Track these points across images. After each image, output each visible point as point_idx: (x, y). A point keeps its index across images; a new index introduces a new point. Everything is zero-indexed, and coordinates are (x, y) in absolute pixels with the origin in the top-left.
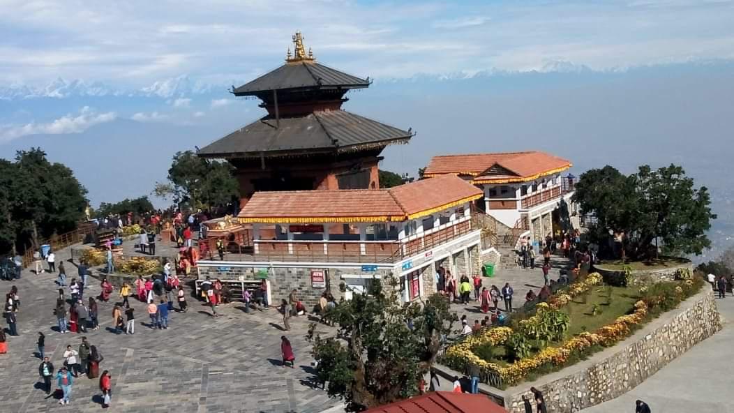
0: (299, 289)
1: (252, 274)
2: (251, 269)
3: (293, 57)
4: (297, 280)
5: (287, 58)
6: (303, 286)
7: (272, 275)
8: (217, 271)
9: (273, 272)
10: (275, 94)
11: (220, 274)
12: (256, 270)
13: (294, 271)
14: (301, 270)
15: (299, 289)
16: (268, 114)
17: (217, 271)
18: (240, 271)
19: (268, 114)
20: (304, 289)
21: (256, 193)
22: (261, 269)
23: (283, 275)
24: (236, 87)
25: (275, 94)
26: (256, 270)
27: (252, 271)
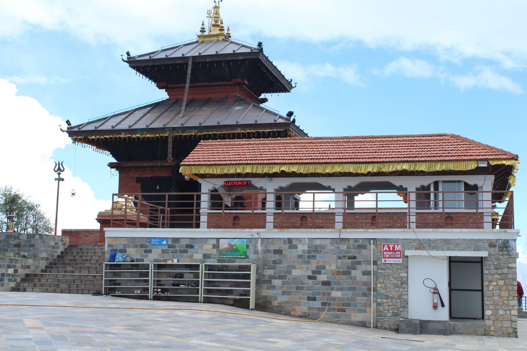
0: (310, 278)
1: (214, 251)
2: (214, 242)
3: (206, 33)
4: (308, 262)
5: (200, 33)
6: (319, 273)
7: (256, 252)
8: (142, 246)
9: (260, 248)
10: (190, 63)
11: (150, 251)
12: (224, 244)
13: (302, 248)
14: (318, 242)
15: (310, 278)
16: (168, 97)
17: (142, 246)
18: (192, 247)
19: (168, 97)
20: (322, 278)
21: (202, 141)
22: (234, 242)
23: (279, 252)
24: (132, 55)
25: (190, 63)
26: (224, 244)
27: (216, 246)
